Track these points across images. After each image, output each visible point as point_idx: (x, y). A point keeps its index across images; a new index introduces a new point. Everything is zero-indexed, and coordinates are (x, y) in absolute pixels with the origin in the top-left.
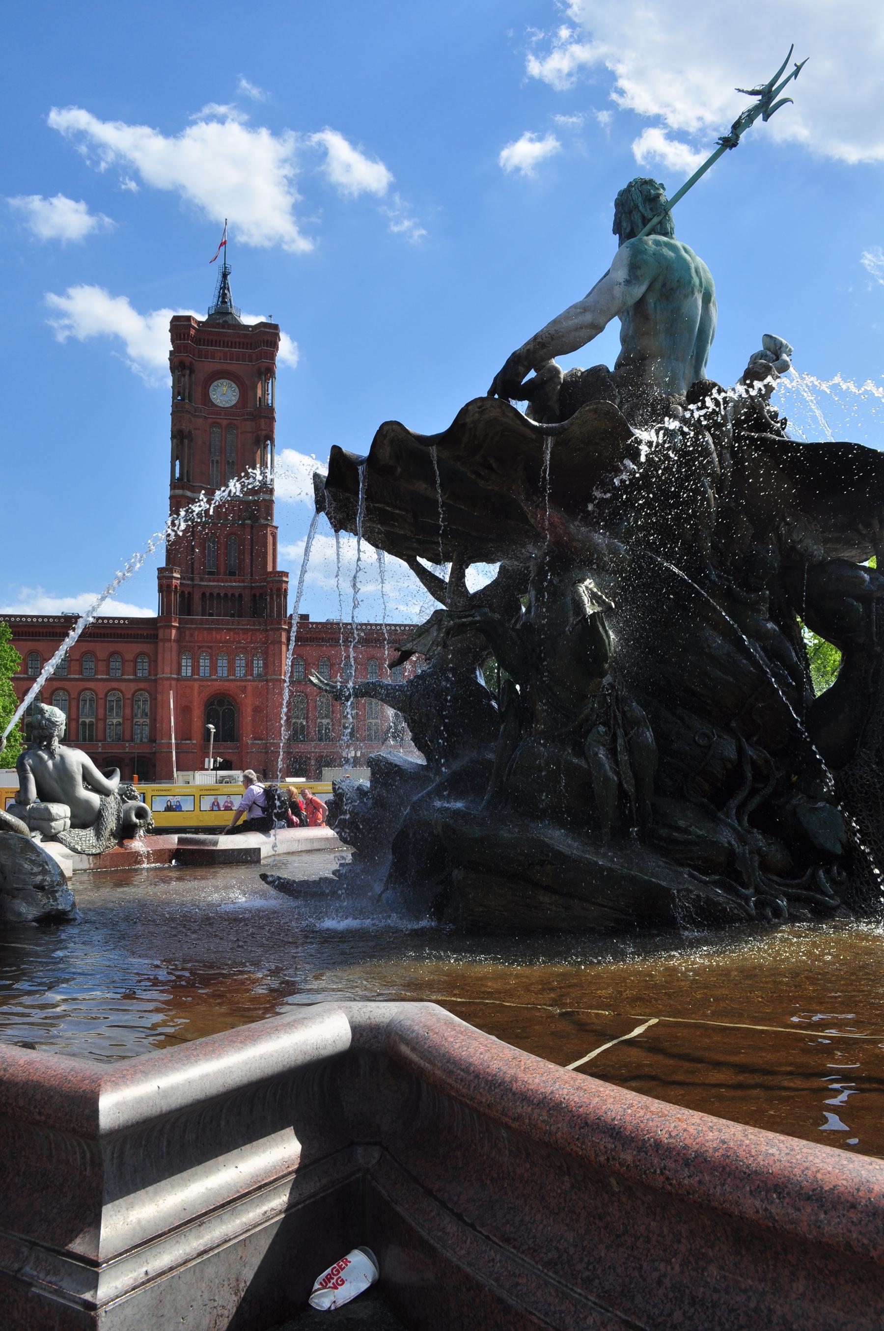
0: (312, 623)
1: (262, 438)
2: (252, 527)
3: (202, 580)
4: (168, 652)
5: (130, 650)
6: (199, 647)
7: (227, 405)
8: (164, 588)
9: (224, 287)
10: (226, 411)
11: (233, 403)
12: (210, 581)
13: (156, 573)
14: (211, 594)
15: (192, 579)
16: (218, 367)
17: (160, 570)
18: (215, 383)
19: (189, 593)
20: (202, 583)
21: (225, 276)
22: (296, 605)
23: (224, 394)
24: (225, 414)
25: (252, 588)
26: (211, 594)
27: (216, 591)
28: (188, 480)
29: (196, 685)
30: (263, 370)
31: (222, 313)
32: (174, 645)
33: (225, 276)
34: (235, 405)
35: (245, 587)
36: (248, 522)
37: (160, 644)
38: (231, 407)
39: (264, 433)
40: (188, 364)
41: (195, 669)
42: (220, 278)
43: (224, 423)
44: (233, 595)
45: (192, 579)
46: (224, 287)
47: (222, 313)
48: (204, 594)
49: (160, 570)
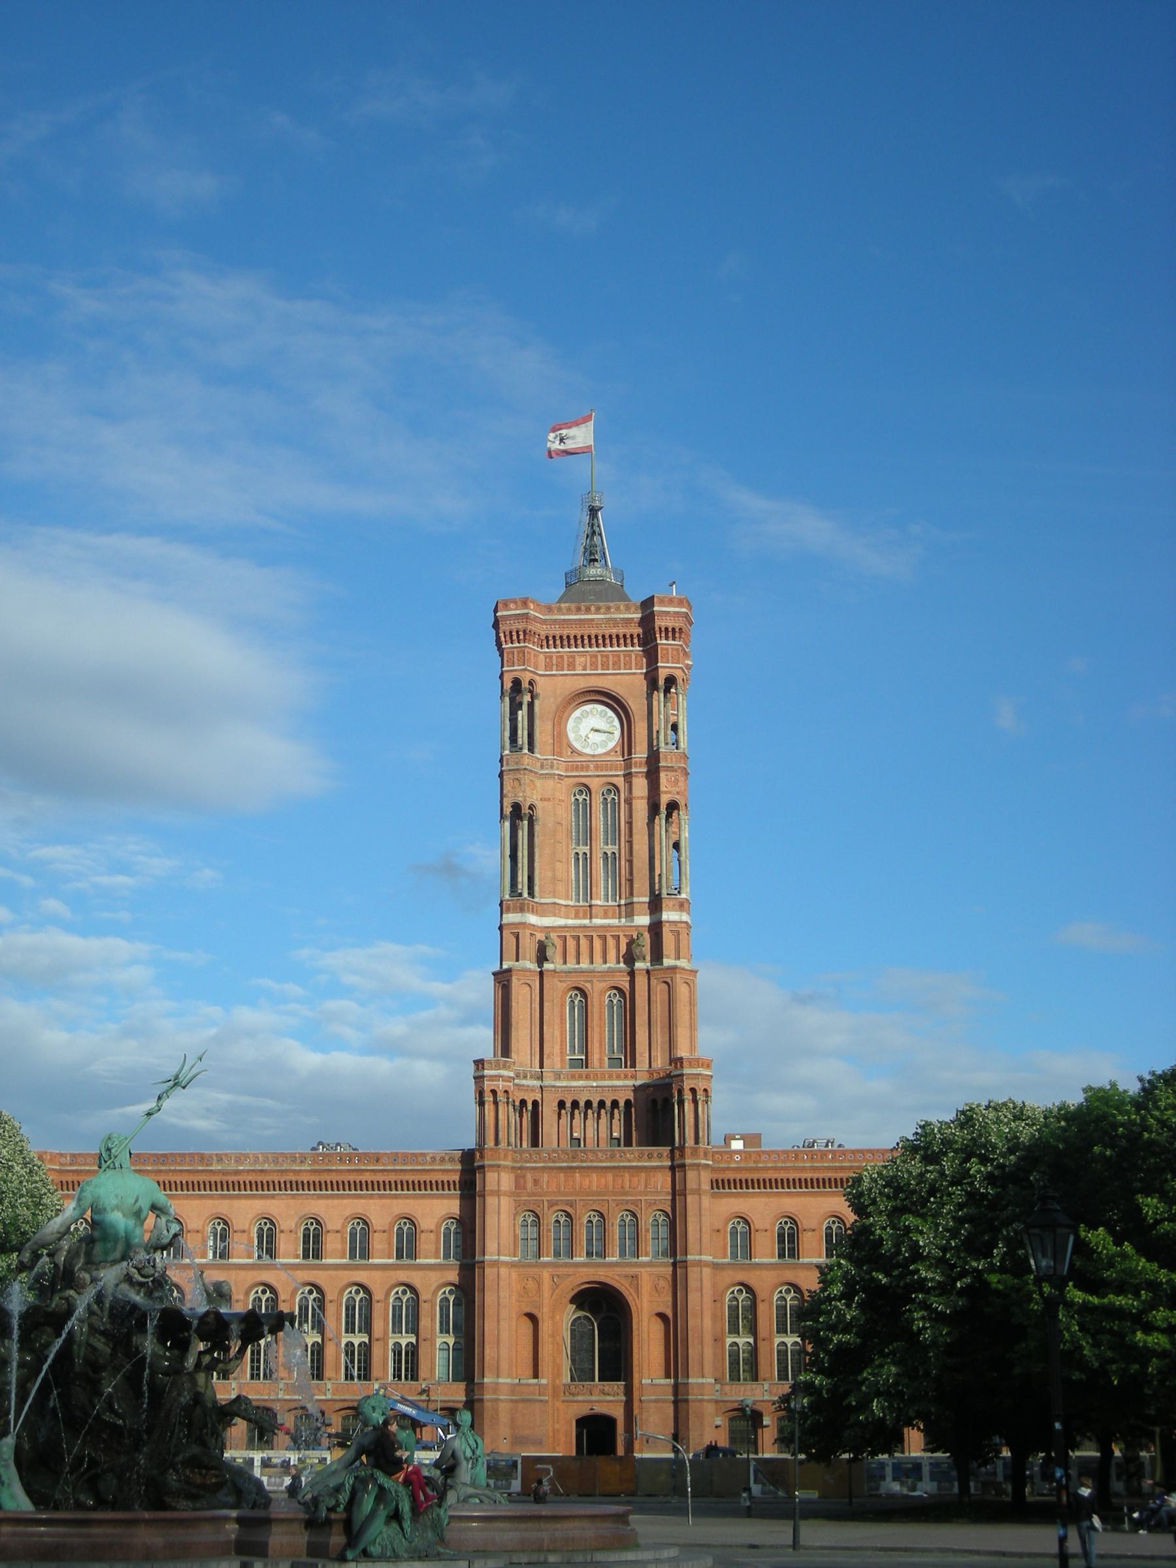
3: (558, 1076)
6: (552, 1204)
7: (600, 751)
10: (598, 763)
11: (611, 745)
12: (573, 1078)
15: (541, 1078)
17: (479, 1064)
18: (577, 713)
19: (535, 1103)
20: (558, 1084)
21: (593, 512)
23: (593, 731)
24: (597, 768)
28: (531, 893)
30: (661, 682)
32: (505, 1201)
34: (613, 750)
38: (607, 754)
40: (525, 685)
45: (541, 1078)
48: (562, 1105)
49: (479, 1064)
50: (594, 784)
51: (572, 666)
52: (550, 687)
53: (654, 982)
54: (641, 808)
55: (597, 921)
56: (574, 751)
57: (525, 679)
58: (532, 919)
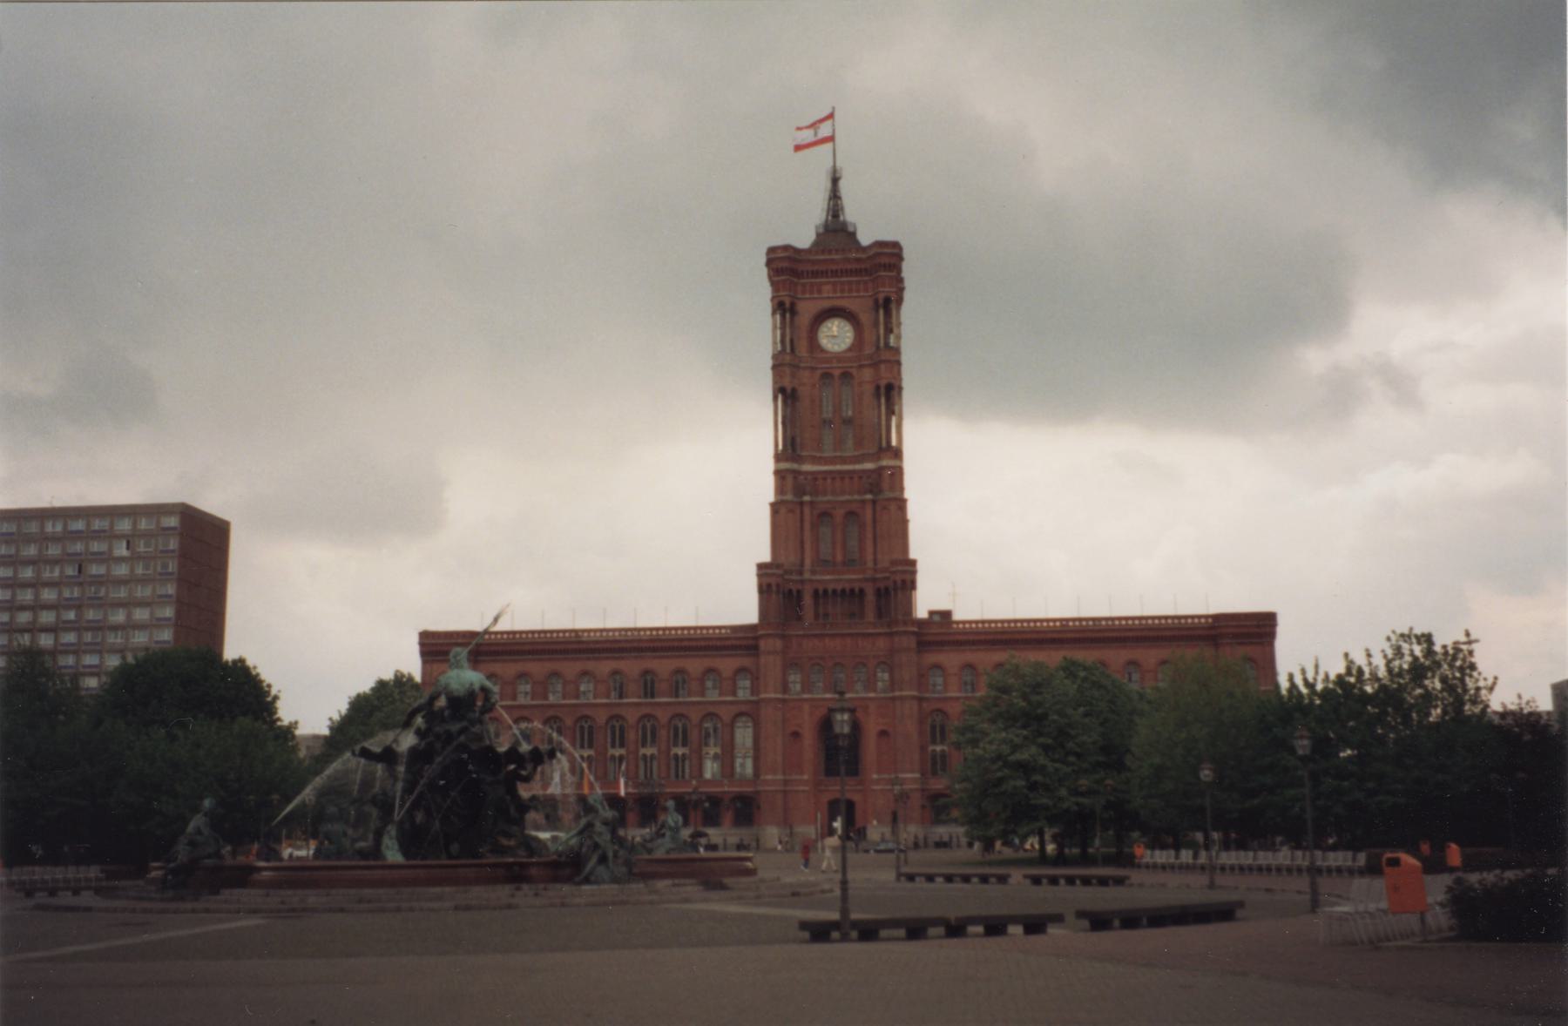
0: (958, 623)
1: (883, 391)
2: (874, 502)
3: (813, 572)
4: (771, 664)
5: (727, 665)
8: (764, 590)
9: (835, 195)
10: (838, 357)
13: (753, 571)
14: (825, 591)
15: (801, 573)
16: (827, 304)
17: (761, 567)
21: (835, 181)
22: (925, 602)
23: (836, 336)
25: (874, 580)
26: (825, 591)
27: (830, 587)
29: (806, 707)
31: (836, 229)
33: (835, 181)
34: (850, 349)
35: (866, 580)
36: (869, 496)
37: (763, 659)
39: (883, 383)
40: (788, 305)
41: (807, 686)
42: (829, 185)
43: (837, 373)
44: (852, 590)
46: (835, 195)
47: (836, 229)
48: (816, 592)
49: (761, 567)
50: (837, 373)
51: (820, 292)
52: (807, 309)
53: (878, 508)
54: (868, 389)
55: (838, 467)
56: (823, 351)
57: (787, 302)
58: (795, 466)
